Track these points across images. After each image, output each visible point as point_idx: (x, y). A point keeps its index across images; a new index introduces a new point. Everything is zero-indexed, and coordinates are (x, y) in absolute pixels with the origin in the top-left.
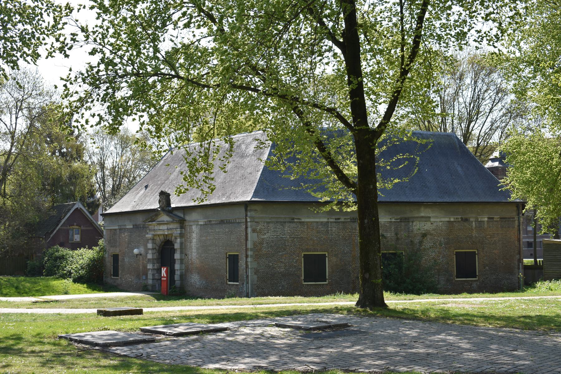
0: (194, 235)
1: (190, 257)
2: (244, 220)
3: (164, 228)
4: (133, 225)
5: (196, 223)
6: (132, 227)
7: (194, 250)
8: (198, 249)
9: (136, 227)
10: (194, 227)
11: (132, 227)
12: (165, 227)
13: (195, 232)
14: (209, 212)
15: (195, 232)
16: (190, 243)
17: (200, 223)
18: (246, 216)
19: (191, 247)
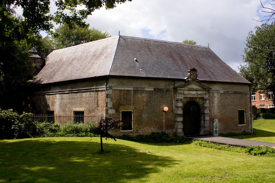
0: (216, 99)
1: (212, 112)
2: (249, 93)
3: (193, 92)
4: (155, 89)
5: (218, 92)
6: (153, 90)
7: (215, 108)
8: (218, 107)
9: (157, 90)
10: (216, 94)
11: (153, 90)
12: (194, 93)
13: (217, 97)
14: (227, 86)
15: (217, 97)
16: (213, 103)
17: (221, 92)
18: (250, 91)
19: (214, 106)
